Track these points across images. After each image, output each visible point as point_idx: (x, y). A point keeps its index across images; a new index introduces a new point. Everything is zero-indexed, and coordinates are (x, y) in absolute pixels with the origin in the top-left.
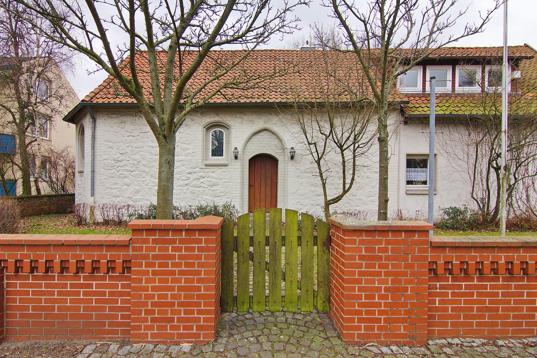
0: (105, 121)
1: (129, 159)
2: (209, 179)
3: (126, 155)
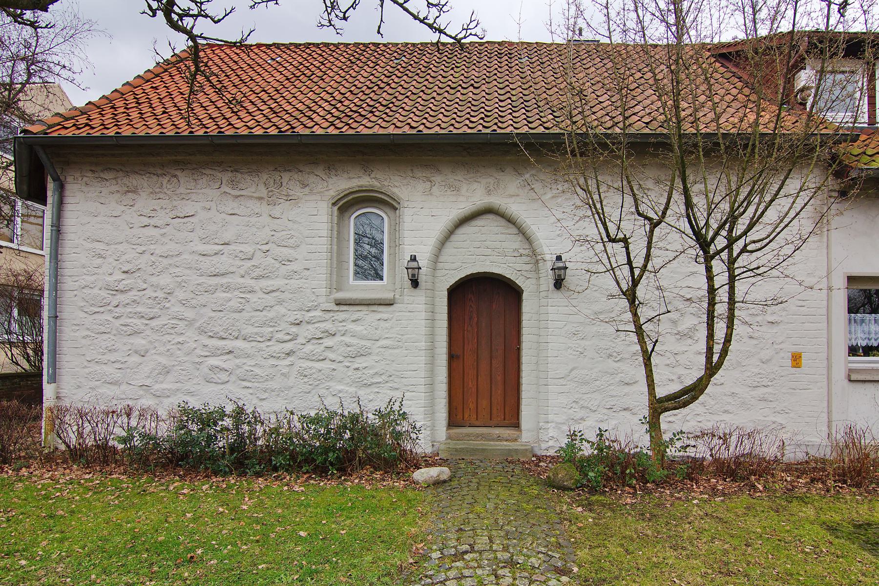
1: (145, 286)
2: (347, 339)
3: (137, 275)
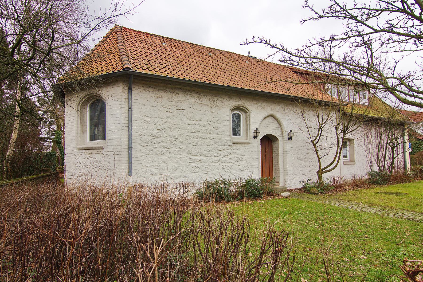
0: (140, 94)
1: (166, 135)
2: (236, 155)
3: (164, 131)
